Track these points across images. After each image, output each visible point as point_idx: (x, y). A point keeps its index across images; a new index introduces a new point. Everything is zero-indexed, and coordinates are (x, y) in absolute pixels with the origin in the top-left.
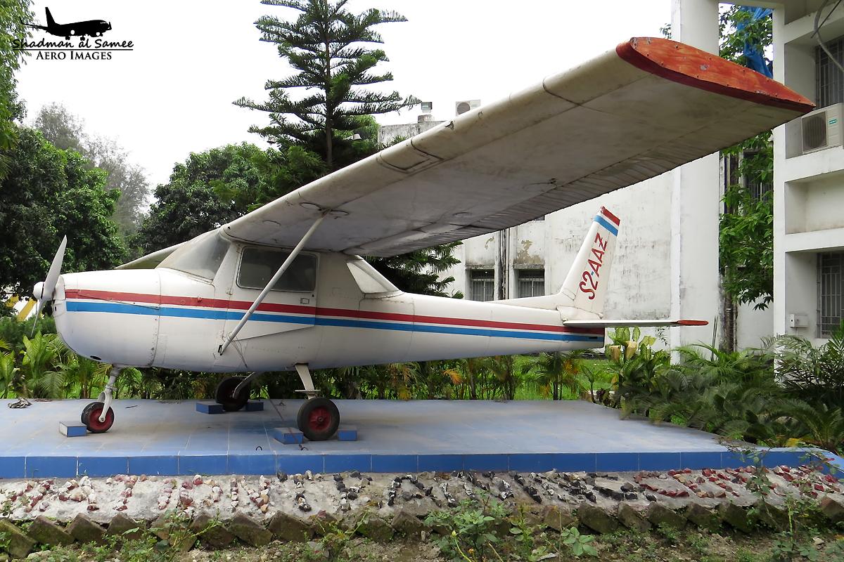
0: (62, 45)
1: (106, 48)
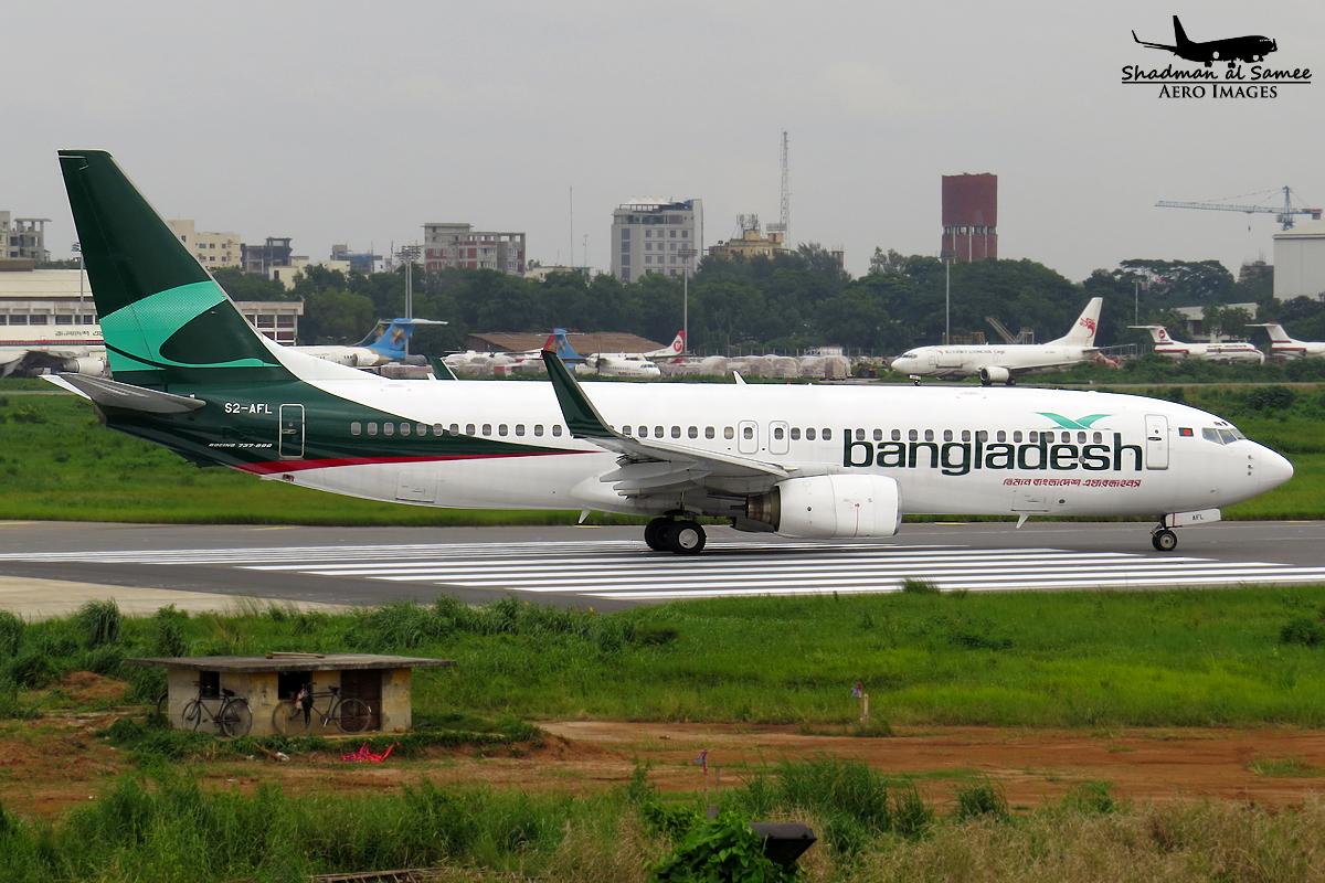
1: (1269, 79)
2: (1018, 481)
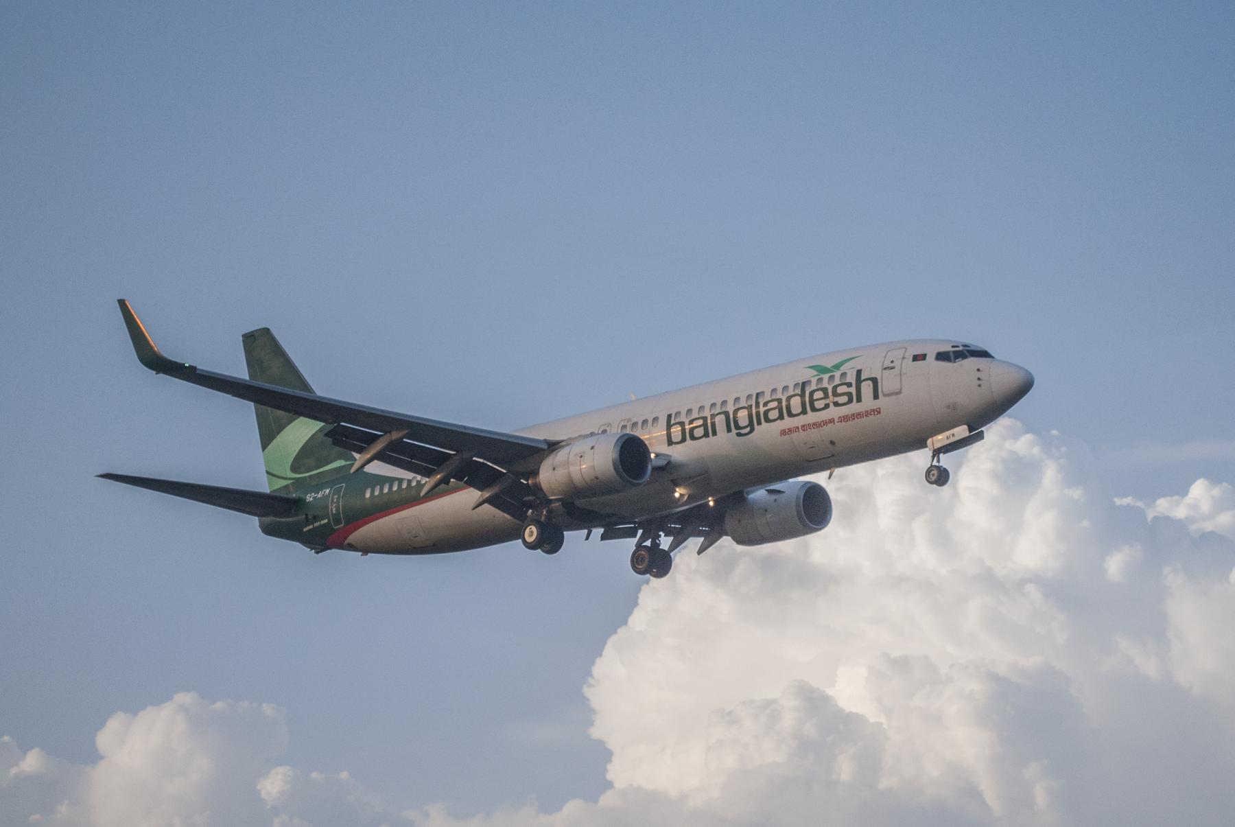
2: (790, 430)
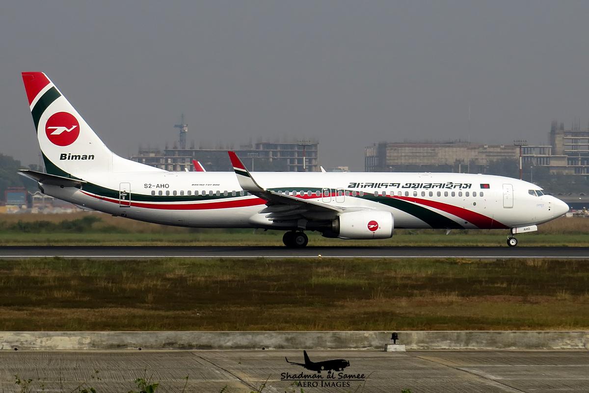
0: (315, 377)
